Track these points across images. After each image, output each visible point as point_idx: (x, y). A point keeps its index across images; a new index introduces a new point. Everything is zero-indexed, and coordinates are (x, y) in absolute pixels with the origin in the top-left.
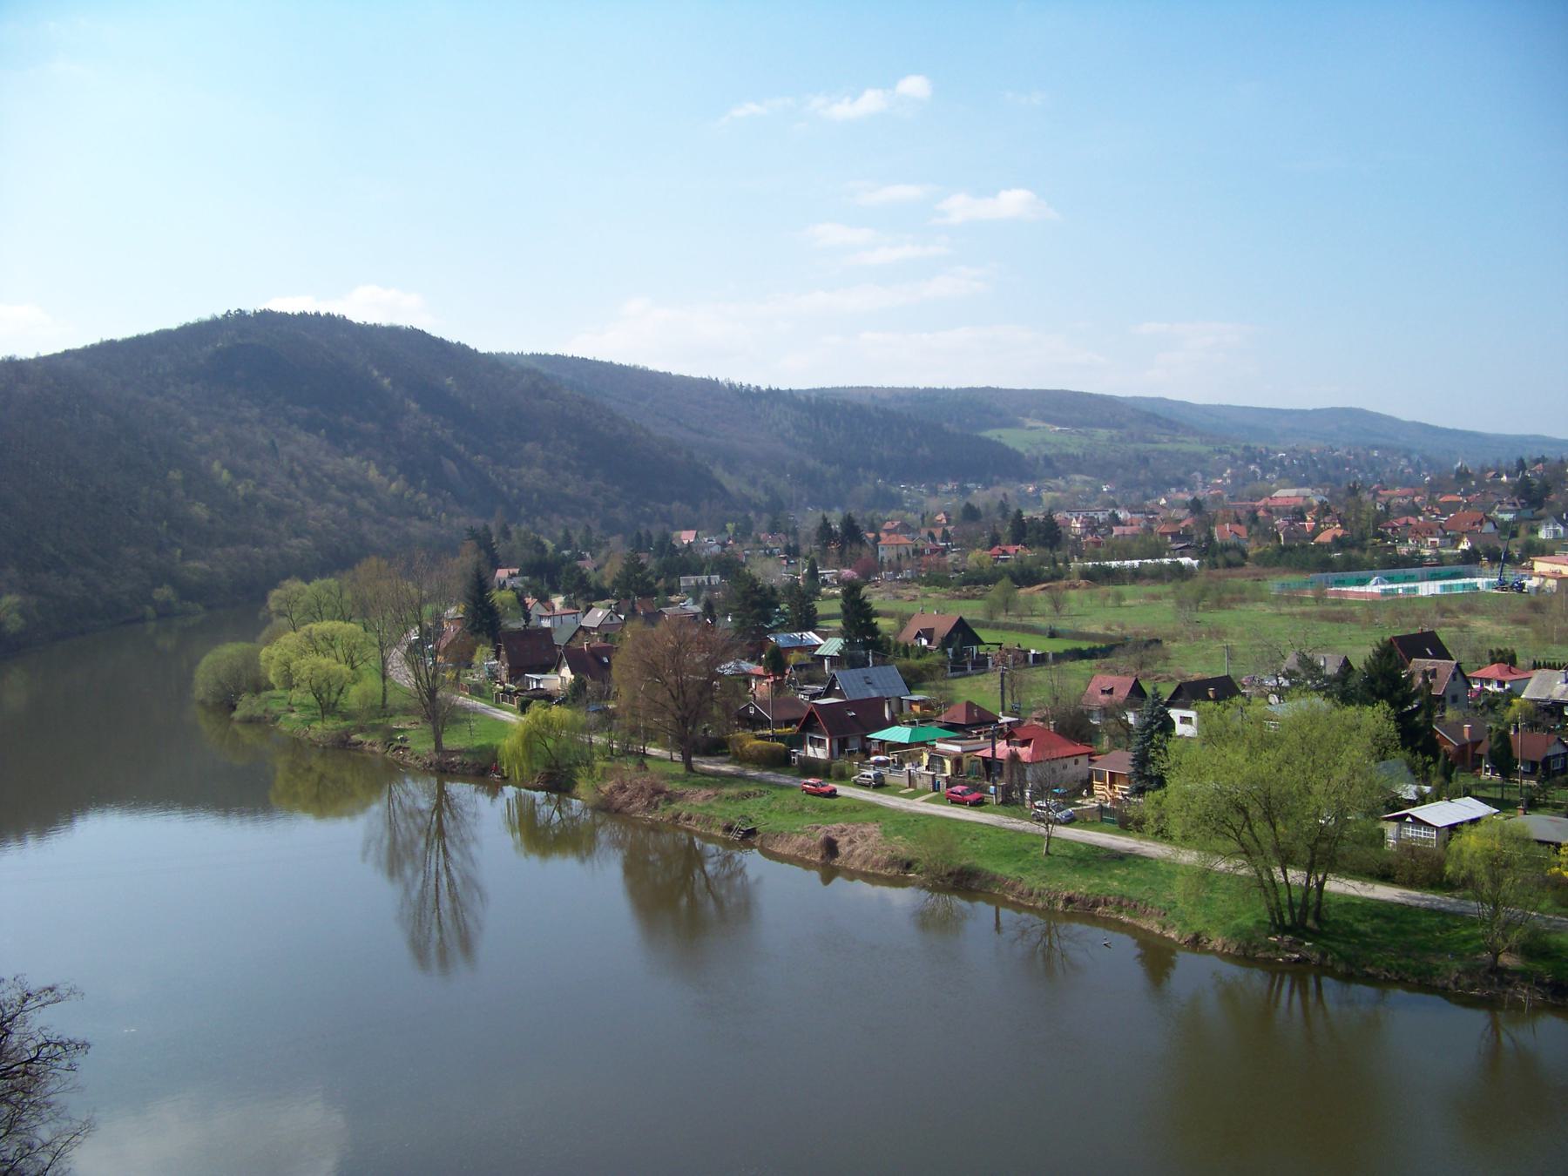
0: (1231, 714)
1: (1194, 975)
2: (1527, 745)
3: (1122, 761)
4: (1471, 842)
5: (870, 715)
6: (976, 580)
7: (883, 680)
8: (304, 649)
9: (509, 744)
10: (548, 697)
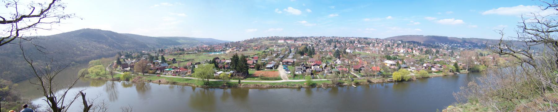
0: (200, 65)
1: (197, 89)
2: (226, 66)
3: (190, 70)
4: (222, 75)
5: (164, 68)
6: (176, 54)
7: (166, 65)
8: (93, 69)
9: (121, 77)
10: (127, 71)
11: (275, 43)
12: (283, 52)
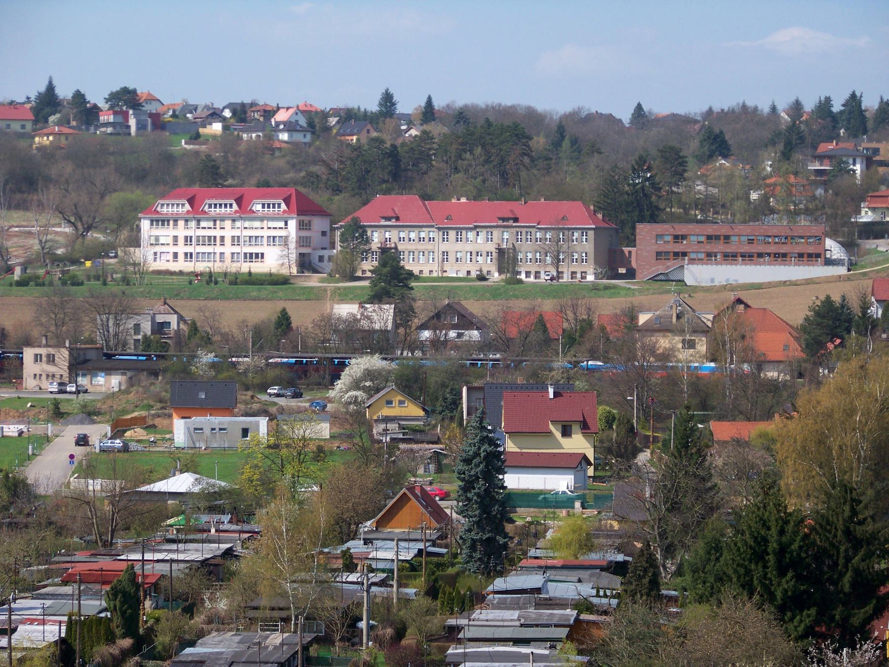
11: (52, 277)
12: (268, 563)
